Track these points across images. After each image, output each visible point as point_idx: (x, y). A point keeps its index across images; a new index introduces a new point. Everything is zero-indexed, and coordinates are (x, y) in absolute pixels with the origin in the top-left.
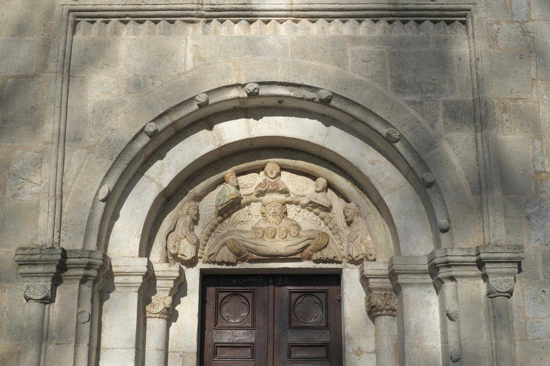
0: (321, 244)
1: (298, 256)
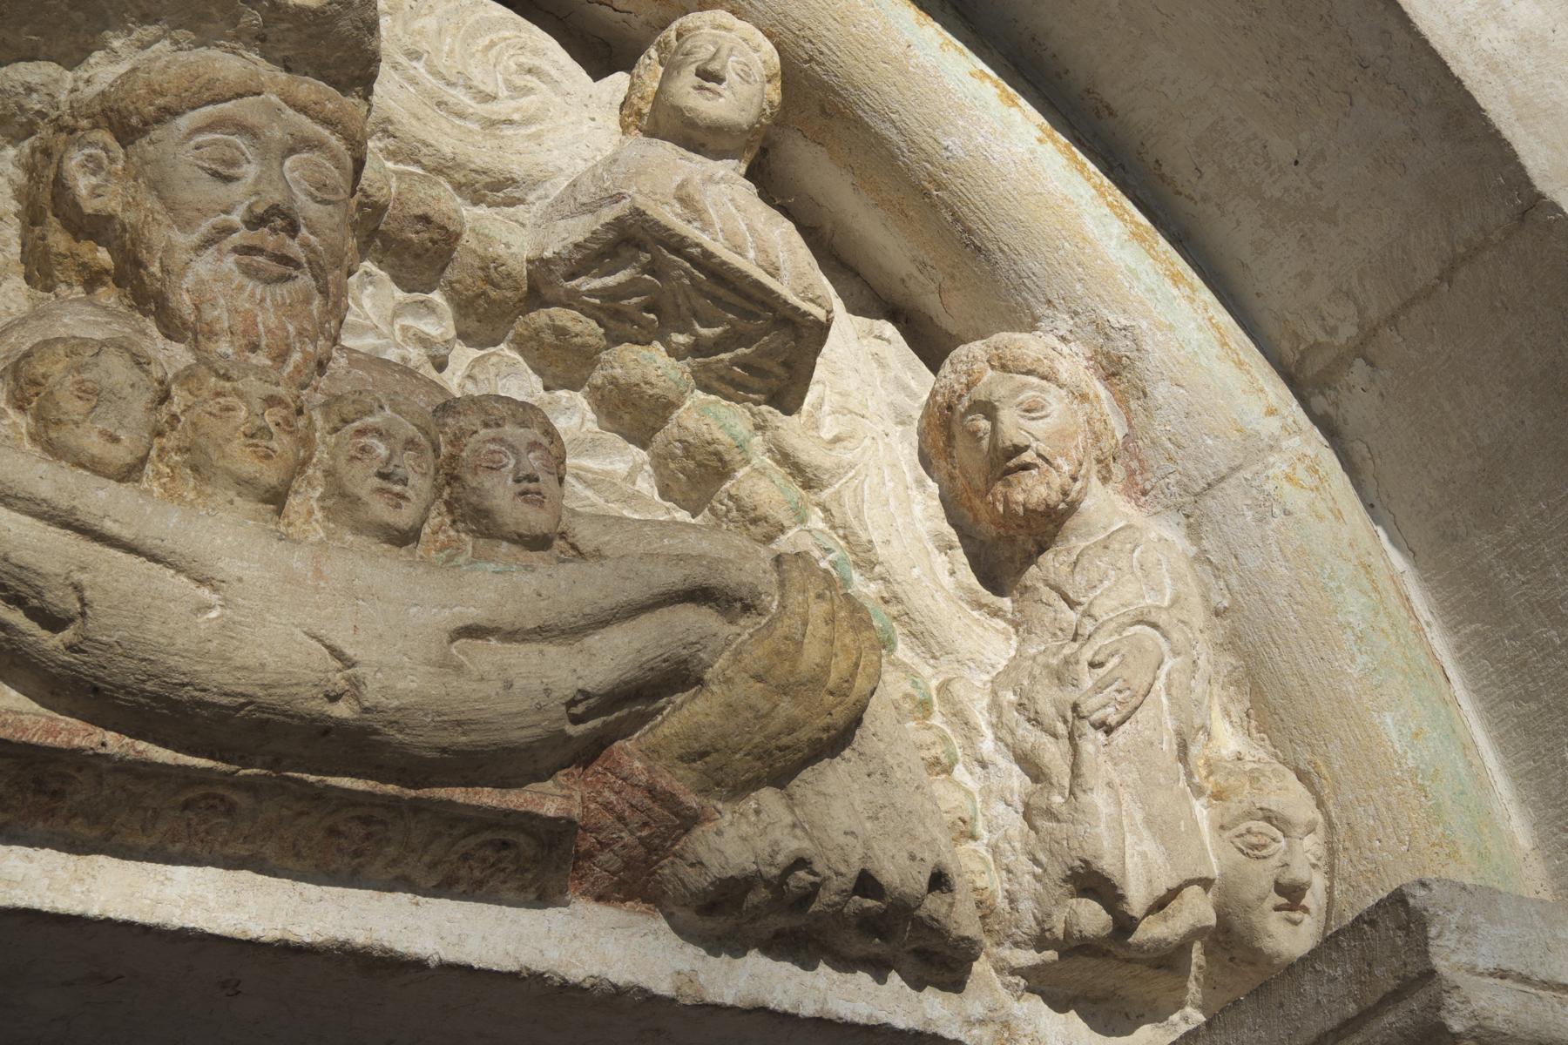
0: (816, 680)
1: (549, 799)
